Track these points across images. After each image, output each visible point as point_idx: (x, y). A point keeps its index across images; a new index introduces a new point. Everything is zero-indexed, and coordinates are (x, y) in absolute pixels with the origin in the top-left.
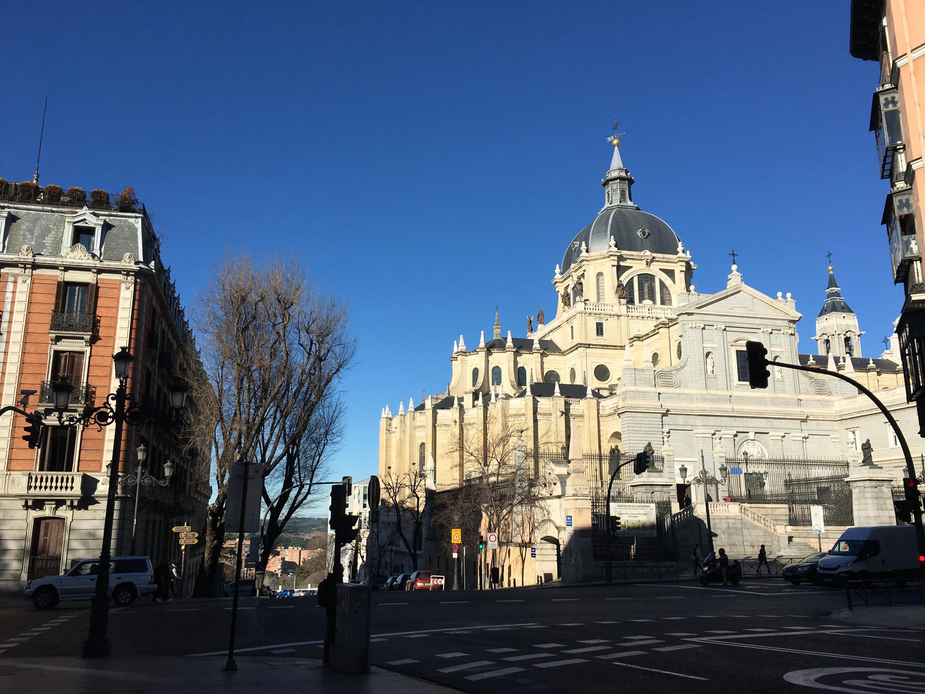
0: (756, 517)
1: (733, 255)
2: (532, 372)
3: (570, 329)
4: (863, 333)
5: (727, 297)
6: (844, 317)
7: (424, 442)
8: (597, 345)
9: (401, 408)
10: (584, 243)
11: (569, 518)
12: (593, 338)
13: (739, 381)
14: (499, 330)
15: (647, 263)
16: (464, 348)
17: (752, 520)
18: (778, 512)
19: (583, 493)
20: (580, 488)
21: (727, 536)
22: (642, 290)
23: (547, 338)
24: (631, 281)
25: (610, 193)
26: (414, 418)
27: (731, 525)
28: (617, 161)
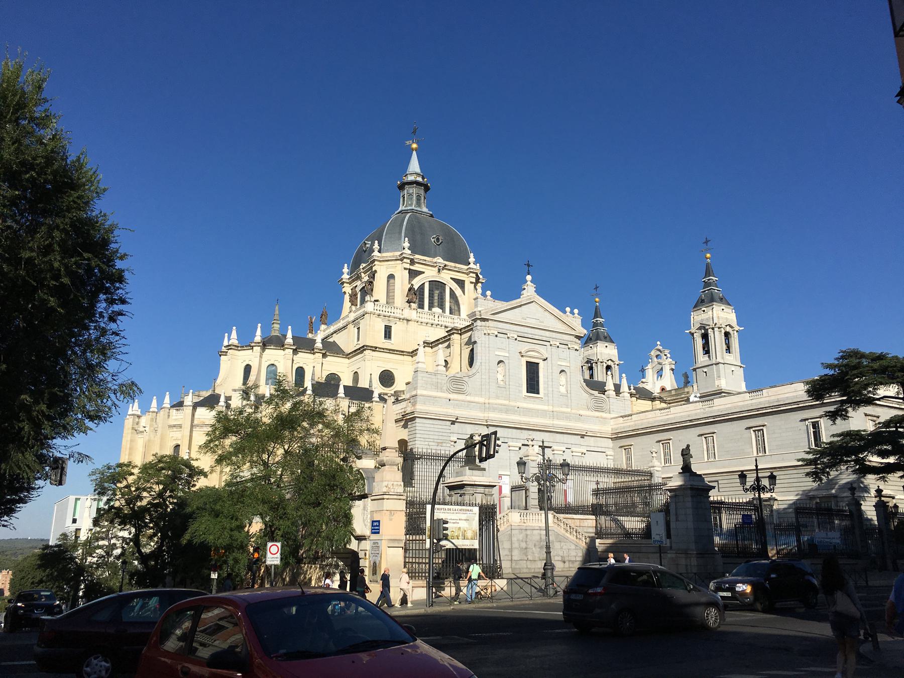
0: (568, 528)
1: (529, 265)
2: (313, 371)
3: (356, 330)
4: (621, 362)
5: (520, 306)
6: (606, 346)
7: (179, 443)
8: (383, 349)
9: (154, 403)
10: (376, 242)
11: (375, 524)
12: (381, 341)
13: (527, 392)
14: (278, 326)
16: (236, 342)
17: (563, 532)
19: (396, 491)
20: (393, 484)
21: (539, 549)
22: (432, 297)
23: (331, 340)
24: (421, 287)
25: (405, 196)
26: (169, 416)
28: (414, 166)
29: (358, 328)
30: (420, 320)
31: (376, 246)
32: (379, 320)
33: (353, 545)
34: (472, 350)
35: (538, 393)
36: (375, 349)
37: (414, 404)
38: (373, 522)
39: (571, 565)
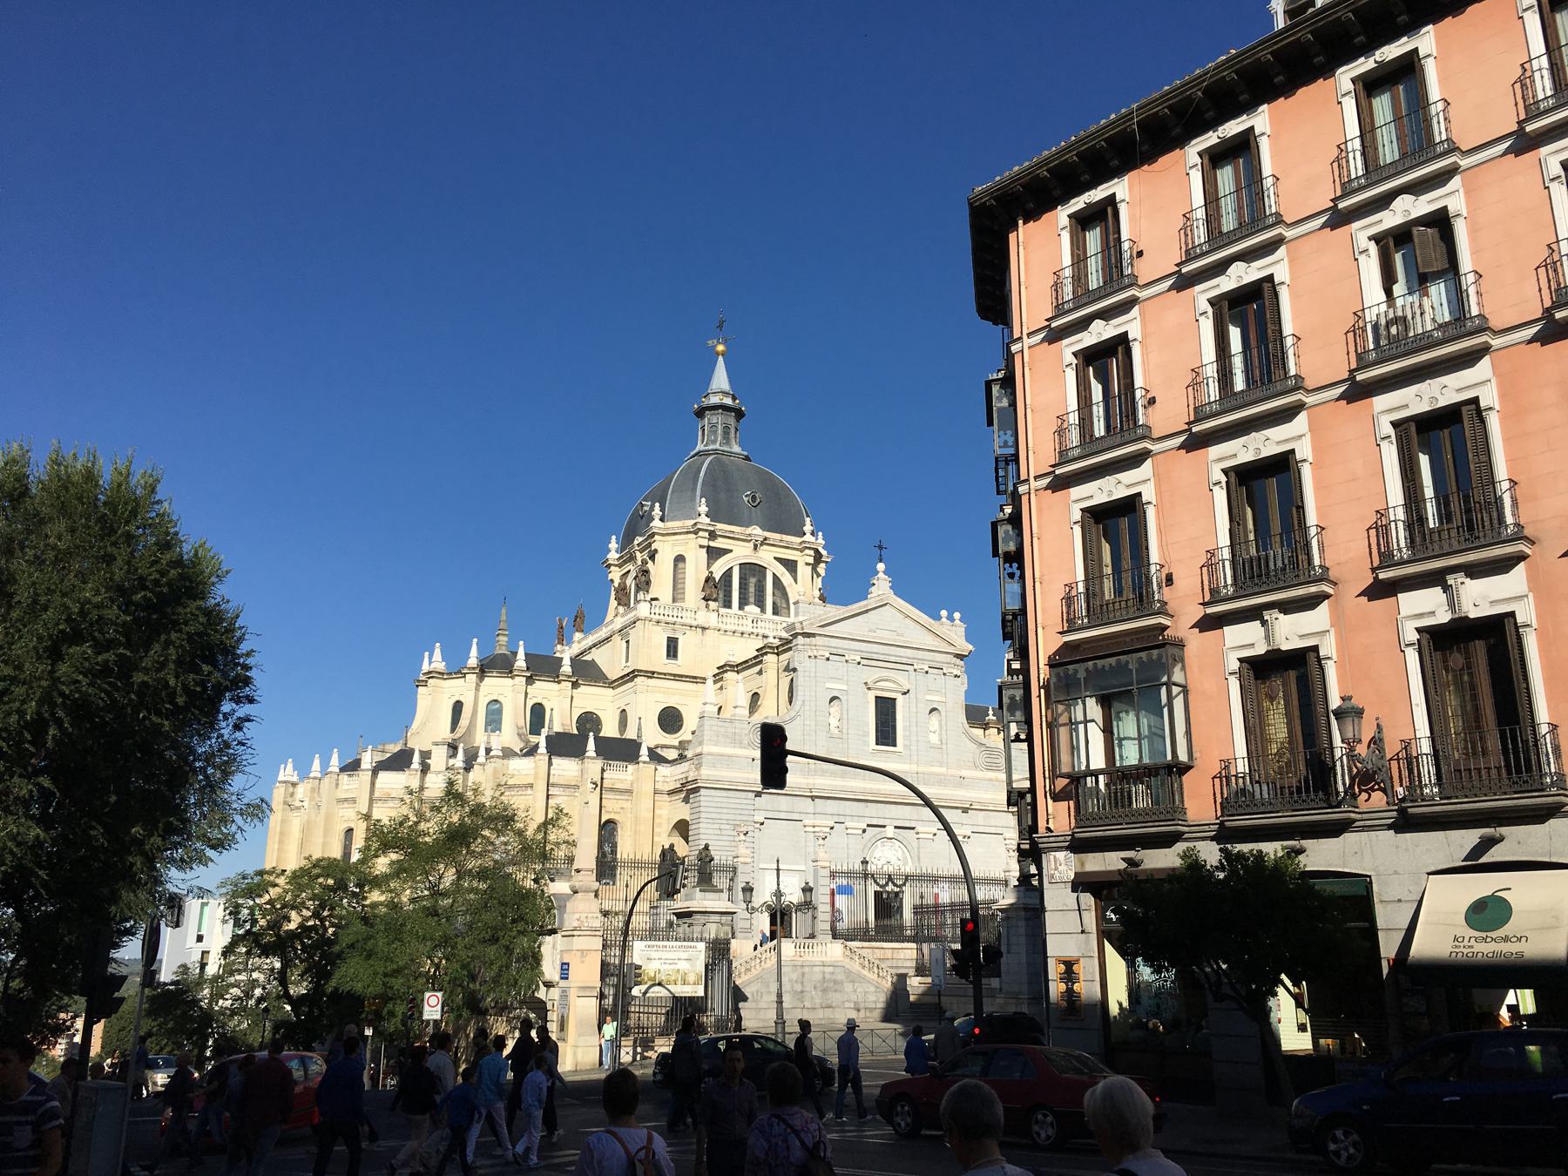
0: (867, 963)
1: (880, 547)
5: (867, 611)
7: (352, 825)
8: (665, 674)
9: (316, 765)
10: (657, 505)
12: (660, 662)
13: (877, 744)
14: (505, 639)
15: (755, 547)
17: (860, 968)
18: (902, 954)
21: (820, 993)
26: (337, 785)
27: (827, 976)
28: (720, 379)
29: (628, 642)
30: (724, 627)
31: (657, 511)
32: (658, 629)
33: (542, 993)
34: (792, 680)
35: (895, 746)
36: (651, 674)
37: (698, 767)
38: (563, 964)
39: (868, 1014)
